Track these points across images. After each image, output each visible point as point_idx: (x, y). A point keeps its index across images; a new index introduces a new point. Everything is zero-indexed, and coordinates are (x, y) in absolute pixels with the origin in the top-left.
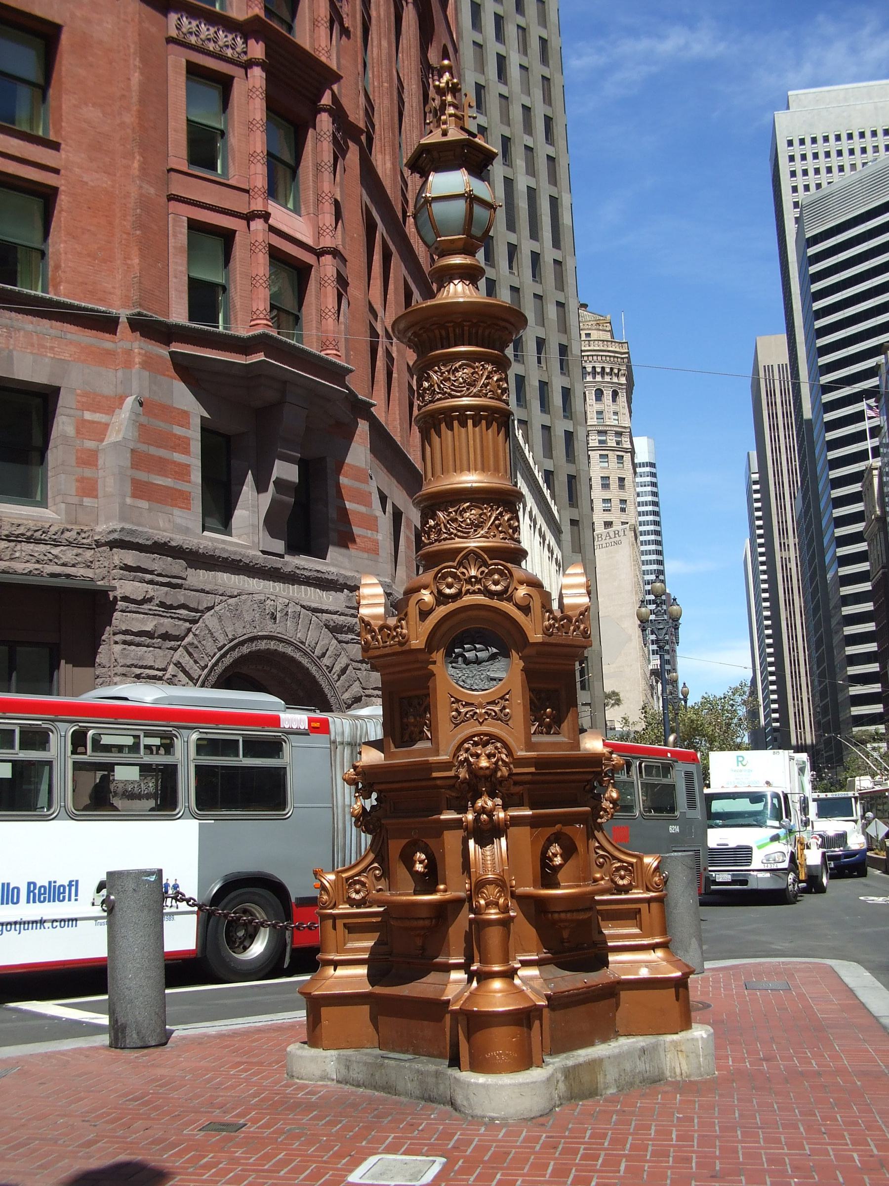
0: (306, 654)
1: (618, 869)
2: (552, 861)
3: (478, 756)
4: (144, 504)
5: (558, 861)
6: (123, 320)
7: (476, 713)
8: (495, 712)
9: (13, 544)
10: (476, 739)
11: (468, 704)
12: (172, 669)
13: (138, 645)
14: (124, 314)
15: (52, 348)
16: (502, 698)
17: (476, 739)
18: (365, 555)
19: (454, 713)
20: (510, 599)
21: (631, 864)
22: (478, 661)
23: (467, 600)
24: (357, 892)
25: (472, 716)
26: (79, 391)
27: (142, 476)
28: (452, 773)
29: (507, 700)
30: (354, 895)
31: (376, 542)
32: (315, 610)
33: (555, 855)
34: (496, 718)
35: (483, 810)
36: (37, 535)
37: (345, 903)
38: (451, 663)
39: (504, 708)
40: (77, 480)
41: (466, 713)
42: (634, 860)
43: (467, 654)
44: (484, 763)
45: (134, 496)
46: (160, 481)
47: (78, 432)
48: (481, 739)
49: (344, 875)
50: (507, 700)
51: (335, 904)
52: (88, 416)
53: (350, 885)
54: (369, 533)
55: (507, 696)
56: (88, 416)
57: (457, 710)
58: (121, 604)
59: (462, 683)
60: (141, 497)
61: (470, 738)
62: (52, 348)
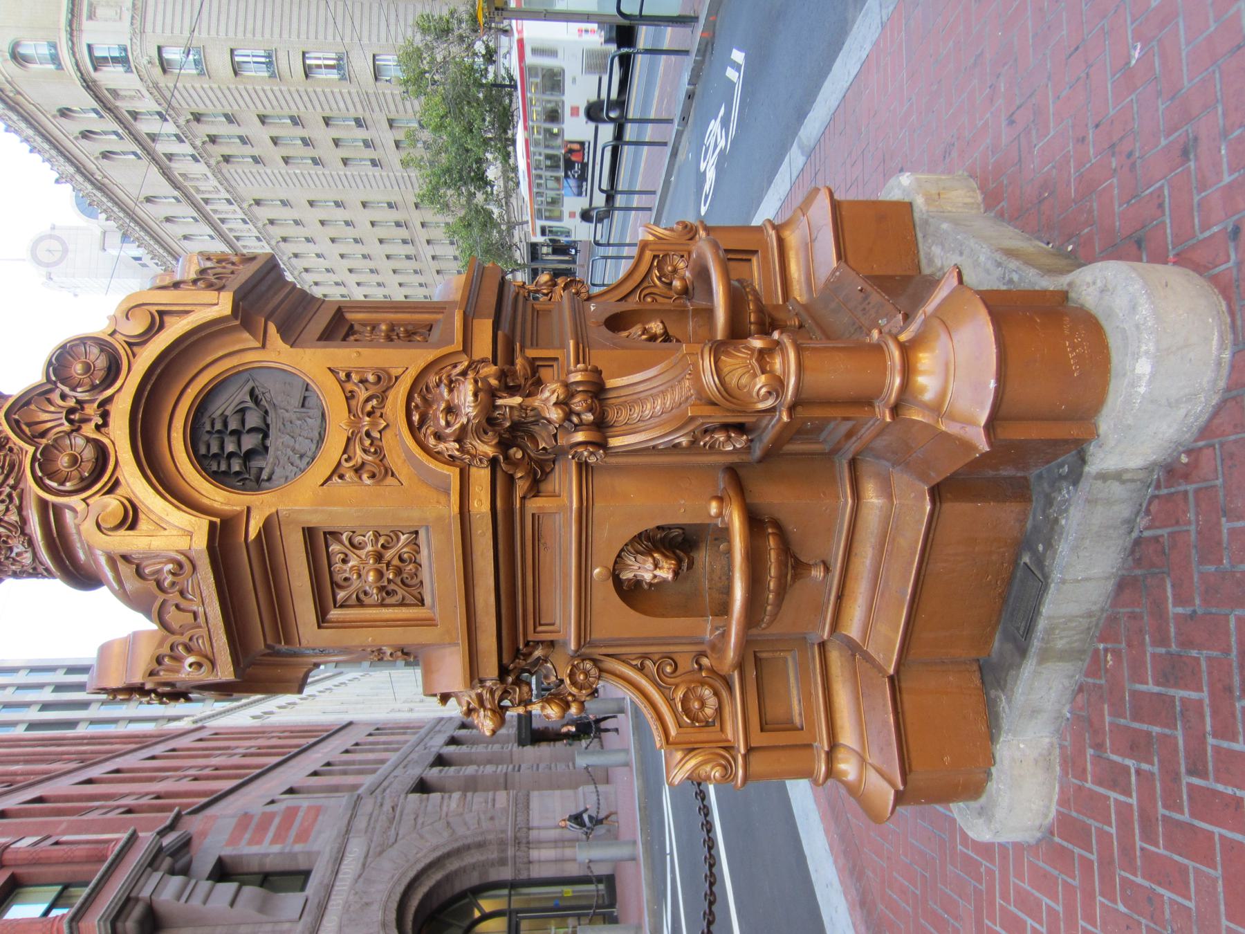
0: (403, 874)
3: (450, 410)
8: (368, 400)
10: (416, 418)
17: (416, 418)
18: (320, 818)
19: (365, 476)
21: (655, 257)
22: (264, 431)
23: (119, 435)
24: (703, 704)
28: (481, 477)
29: (348, 376)
30: (709, 711)
31: (310, 808)
32: (364, 865)
33: (645, 331)
34: (382, 397)
37: (722, 729)
38: (258, 480)
39: (363, 381)
41: (365, 451)
43: (245, 448)
44: (466, 398)
48: (417, 407)
49: (673, 731)
50: (348, 376)
53: (694, 719)
54: (301, 814)
59: (306, 460)
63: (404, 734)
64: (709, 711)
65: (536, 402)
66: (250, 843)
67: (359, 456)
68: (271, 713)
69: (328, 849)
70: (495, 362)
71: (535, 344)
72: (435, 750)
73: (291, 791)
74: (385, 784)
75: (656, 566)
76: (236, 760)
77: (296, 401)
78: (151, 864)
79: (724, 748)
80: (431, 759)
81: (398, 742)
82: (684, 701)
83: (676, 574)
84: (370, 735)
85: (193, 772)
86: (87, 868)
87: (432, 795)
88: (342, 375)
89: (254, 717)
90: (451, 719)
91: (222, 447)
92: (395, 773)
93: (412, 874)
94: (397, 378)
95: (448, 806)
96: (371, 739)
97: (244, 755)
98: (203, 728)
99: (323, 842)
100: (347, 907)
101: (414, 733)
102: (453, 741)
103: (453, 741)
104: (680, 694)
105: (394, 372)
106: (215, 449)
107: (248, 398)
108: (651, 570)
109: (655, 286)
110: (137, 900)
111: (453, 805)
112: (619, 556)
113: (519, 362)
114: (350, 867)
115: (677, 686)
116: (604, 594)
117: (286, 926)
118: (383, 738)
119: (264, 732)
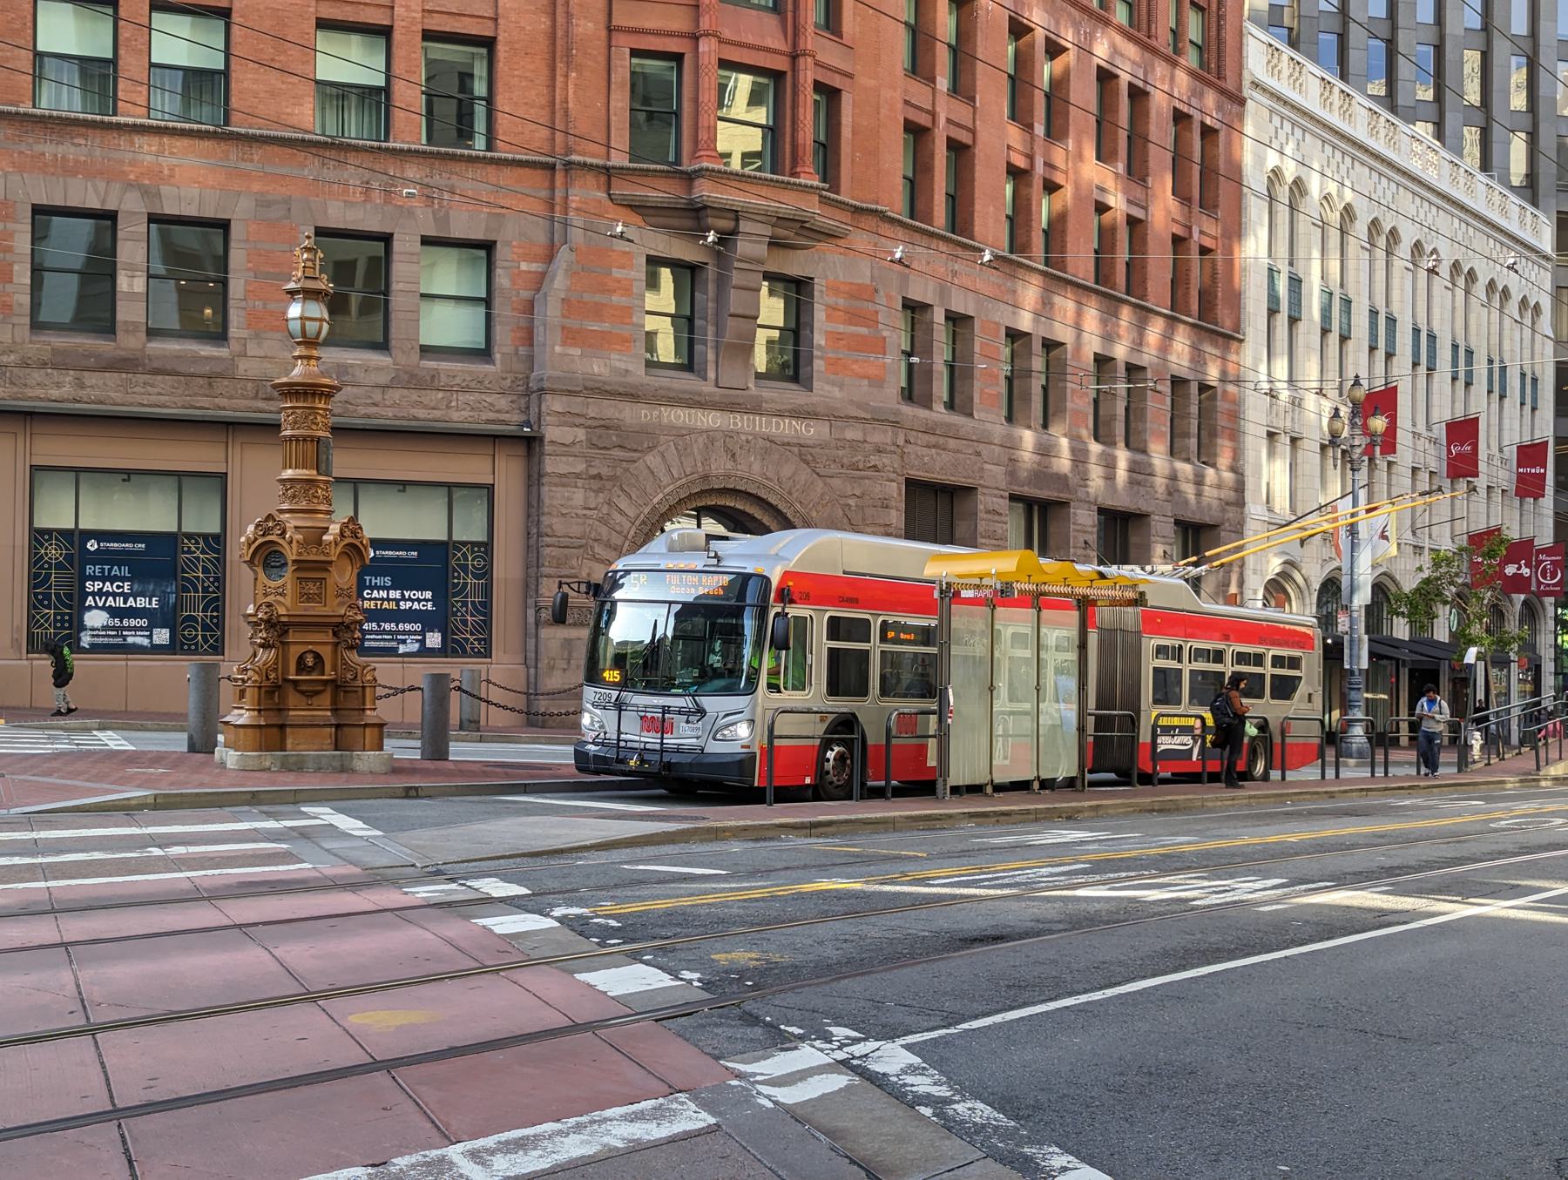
4: (576, 352)
12: (605, 509)
13: (564, 485)
27: (573, 323)
36: (473, 385)
45: (564, 344)
46: (595, 327)
52: (524, 266)
56: (524, 266)
58: (548, 448)
60: (571, 345)
66: (832, 308)
69: (815, 399)
93: (773, 500)
99: (825, 389)
100: (730, 435)
108: (310, 661)
110: (737, 220)
114: (787, 428)
116: (303, 649)
117: (711, 375)
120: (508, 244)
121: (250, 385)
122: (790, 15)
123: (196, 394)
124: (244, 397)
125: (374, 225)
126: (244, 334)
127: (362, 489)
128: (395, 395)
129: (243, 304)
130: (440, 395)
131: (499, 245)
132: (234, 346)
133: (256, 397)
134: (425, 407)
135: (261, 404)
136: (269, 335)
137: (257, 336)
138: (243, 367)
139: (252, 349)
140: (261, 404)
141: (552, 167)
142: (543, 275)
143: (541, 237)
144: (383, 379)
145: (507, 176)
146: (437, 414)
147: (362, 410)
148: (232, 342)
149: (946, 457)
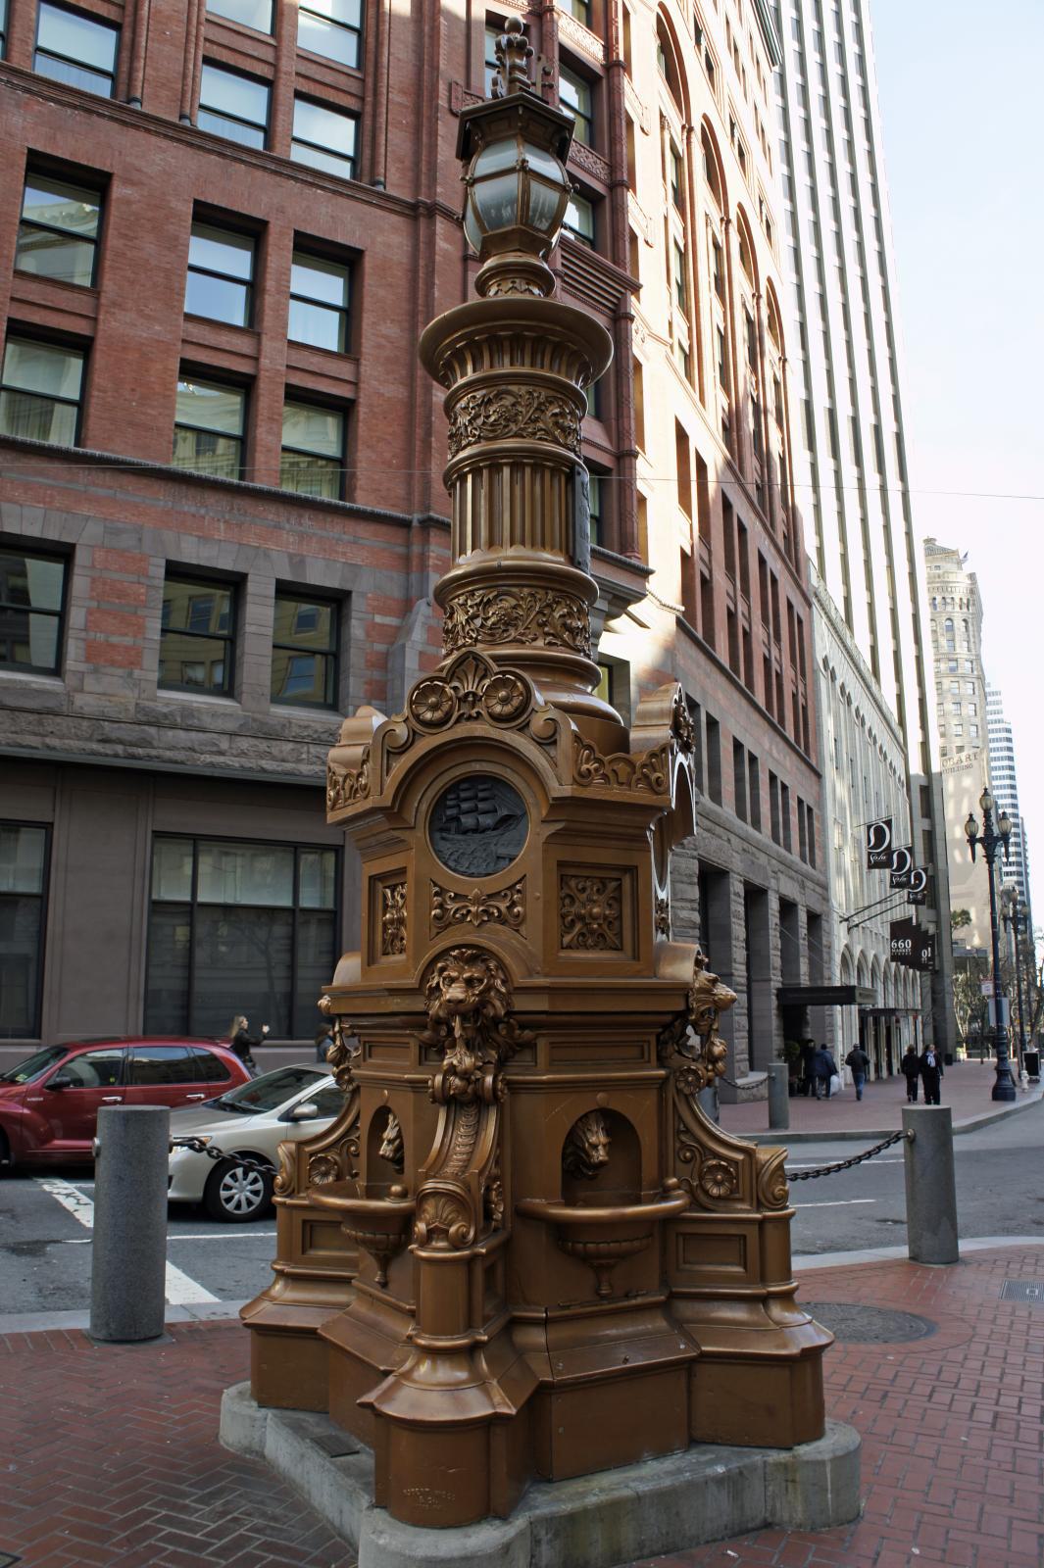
1: (712, 1169)
2: (589, 1156)
3: (453, 980)
5: (601, 1155)
6: (415, 523)
7: (469, 912)
9: (298, 746)
11: (457, 897)
14: (416, 517)
15: (344, 554)
16: (511, 888)
20: (523, 728)
21: (736, 1162)
22: (477, 830)
25: (464, 916)
26: (370, 595)
29: (519, 891)
34: (502, 920)
35: (452, 1070)
36: (324, 737)
38: (442, 830)
39: (513, 904)
40: (366, 683)
42: (740, 1157)
47: (368, 635)
50: (519, 891)
51: (293, 1191)
52: (378, 619)
55: (518, 887)
56: (378, 619)
57: (441, 906)
61: (445, 953)
62: (344, 554)
63: (802, 843)
64: (317, 1180)
65: (460, 1049)
67: (452, 906)
68: (833, 678)
70: (509, 1014)
71: (553, 1046)
72: (773, 883)
73: (713, 724)
74: (719, 830)
75: (390, 1142)
76: (758, 651)
77: (502, 851)
78: (615, 596)
79: (293, 1191)
80: (758, 881)
81: (787, 837)
82: (325, 1160)
83: (383, 1156)
84: (800, 802)
85: (741, 607)
86: (616, 535)
87: (696, 888)
88: (518, 887)
89: (825, 661)
90: (826, 899)
91: (466, 800)
92: (734, 840)
94: (517, 931)
95: (683, 908)
96: (793, 804)
97: (767, 661)
98: (810, 605)
101: (803, 857)
102: (788, 907)
103: (788, 907)
104: (331, 1156)
105: (523, 929)
106: (463, 795)
107: (506, 813)
109: (702, 1162)
111: (684, 914)
112: (586, 1116)
113: (528, 1034)
115: (340, 1155)
118: (794, 819)
119: (803, 674)
120: (363, 595)
121: (85, 723)
122: (614, 422)
123: (22, 732)
124: (79, 738)
125: (226, 563)
126: (82, 667)
127: (202, 846)
128: (244, 744)
129: (83, 635)
130: (291, 746)
131: (354, 595)
132: (71, 680)
133: (89, 739)
134: (274, 758)
135: (95, 746)
136: (111, 670)
137: (96, 671)
138: (80, 700)
139: (90, 683)
140: (95, 746)
141: (405, 524)
142: (398, 628)
143: (396, 592)
144: (231, 726)
145: (364, 530)
146: (288, 766)
147: (208, 758)
148: (68, 677)
149: (715, 842)
